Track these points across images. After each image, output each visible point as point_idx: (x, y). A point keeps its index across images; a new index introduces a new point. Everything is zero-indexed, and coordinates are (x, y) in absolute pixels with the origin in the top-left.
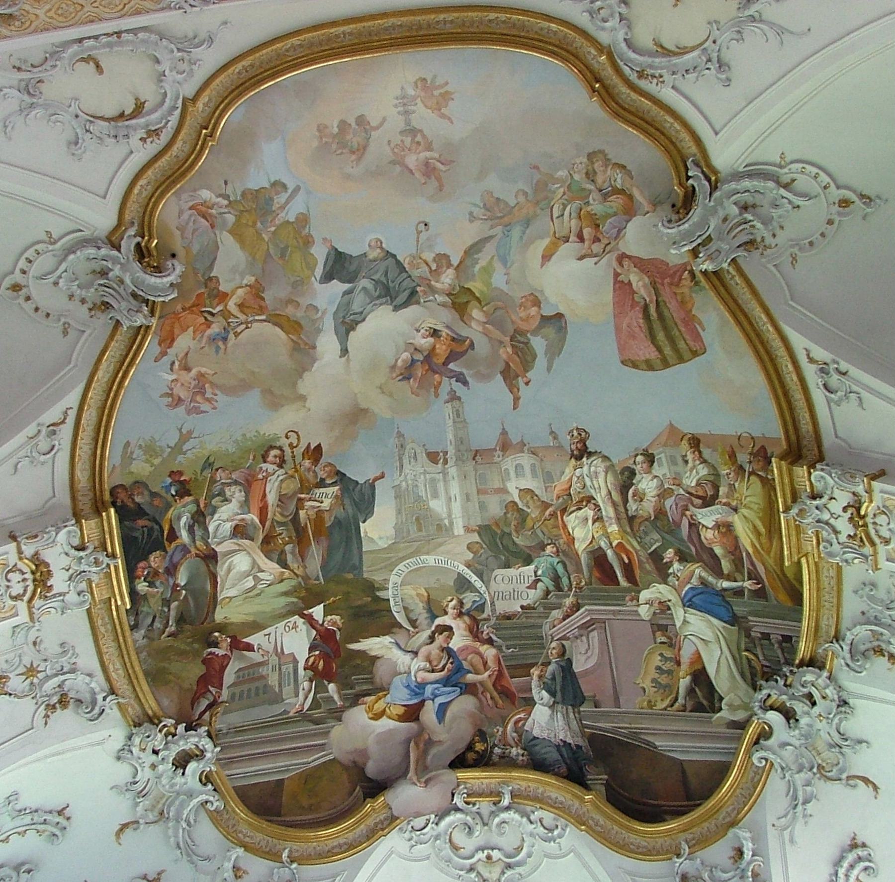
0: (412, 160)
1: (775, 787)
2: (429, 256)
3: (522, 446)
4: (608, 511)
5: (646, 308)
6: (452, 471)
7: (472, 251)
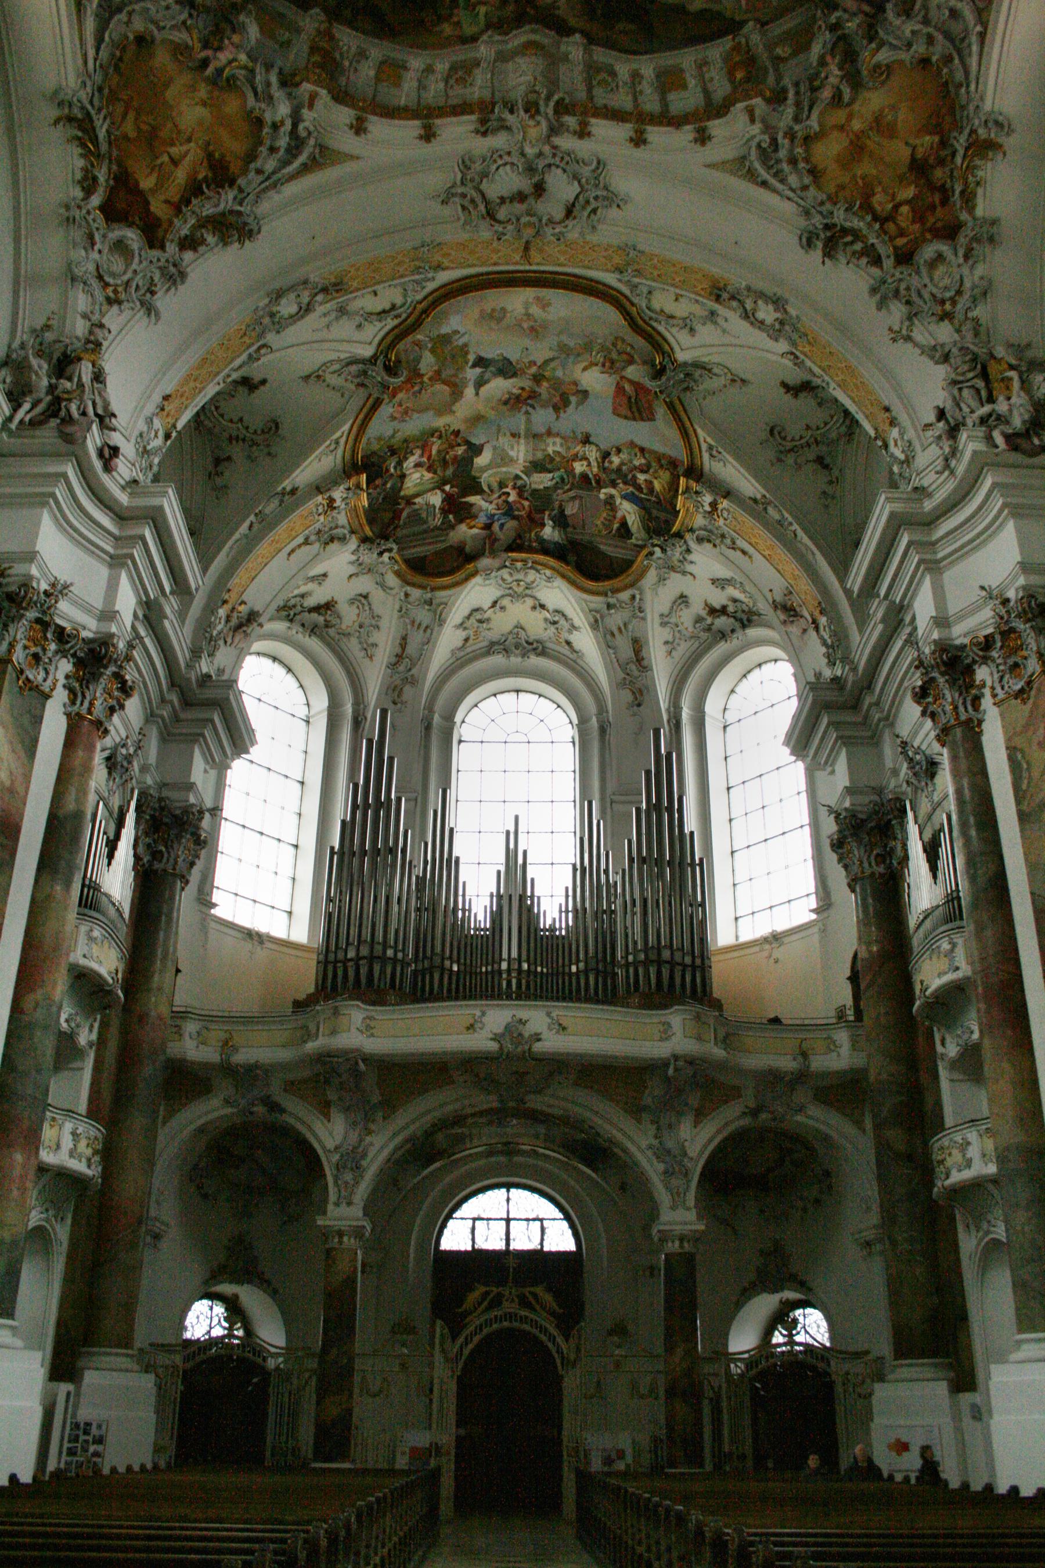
0: (525, 325)
1: (652, 575)
2: (526, 360)
3: (558, 435)
4: (594, 464)
5: (630, 398)
6: (522, 441)
7: (547, 362)
